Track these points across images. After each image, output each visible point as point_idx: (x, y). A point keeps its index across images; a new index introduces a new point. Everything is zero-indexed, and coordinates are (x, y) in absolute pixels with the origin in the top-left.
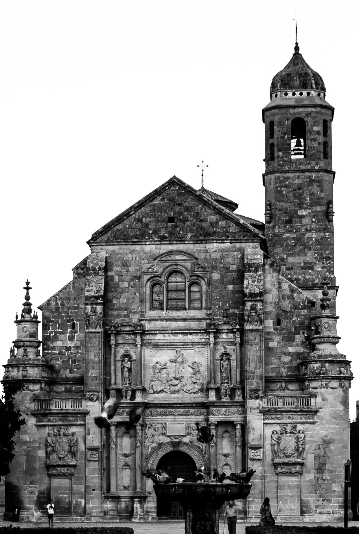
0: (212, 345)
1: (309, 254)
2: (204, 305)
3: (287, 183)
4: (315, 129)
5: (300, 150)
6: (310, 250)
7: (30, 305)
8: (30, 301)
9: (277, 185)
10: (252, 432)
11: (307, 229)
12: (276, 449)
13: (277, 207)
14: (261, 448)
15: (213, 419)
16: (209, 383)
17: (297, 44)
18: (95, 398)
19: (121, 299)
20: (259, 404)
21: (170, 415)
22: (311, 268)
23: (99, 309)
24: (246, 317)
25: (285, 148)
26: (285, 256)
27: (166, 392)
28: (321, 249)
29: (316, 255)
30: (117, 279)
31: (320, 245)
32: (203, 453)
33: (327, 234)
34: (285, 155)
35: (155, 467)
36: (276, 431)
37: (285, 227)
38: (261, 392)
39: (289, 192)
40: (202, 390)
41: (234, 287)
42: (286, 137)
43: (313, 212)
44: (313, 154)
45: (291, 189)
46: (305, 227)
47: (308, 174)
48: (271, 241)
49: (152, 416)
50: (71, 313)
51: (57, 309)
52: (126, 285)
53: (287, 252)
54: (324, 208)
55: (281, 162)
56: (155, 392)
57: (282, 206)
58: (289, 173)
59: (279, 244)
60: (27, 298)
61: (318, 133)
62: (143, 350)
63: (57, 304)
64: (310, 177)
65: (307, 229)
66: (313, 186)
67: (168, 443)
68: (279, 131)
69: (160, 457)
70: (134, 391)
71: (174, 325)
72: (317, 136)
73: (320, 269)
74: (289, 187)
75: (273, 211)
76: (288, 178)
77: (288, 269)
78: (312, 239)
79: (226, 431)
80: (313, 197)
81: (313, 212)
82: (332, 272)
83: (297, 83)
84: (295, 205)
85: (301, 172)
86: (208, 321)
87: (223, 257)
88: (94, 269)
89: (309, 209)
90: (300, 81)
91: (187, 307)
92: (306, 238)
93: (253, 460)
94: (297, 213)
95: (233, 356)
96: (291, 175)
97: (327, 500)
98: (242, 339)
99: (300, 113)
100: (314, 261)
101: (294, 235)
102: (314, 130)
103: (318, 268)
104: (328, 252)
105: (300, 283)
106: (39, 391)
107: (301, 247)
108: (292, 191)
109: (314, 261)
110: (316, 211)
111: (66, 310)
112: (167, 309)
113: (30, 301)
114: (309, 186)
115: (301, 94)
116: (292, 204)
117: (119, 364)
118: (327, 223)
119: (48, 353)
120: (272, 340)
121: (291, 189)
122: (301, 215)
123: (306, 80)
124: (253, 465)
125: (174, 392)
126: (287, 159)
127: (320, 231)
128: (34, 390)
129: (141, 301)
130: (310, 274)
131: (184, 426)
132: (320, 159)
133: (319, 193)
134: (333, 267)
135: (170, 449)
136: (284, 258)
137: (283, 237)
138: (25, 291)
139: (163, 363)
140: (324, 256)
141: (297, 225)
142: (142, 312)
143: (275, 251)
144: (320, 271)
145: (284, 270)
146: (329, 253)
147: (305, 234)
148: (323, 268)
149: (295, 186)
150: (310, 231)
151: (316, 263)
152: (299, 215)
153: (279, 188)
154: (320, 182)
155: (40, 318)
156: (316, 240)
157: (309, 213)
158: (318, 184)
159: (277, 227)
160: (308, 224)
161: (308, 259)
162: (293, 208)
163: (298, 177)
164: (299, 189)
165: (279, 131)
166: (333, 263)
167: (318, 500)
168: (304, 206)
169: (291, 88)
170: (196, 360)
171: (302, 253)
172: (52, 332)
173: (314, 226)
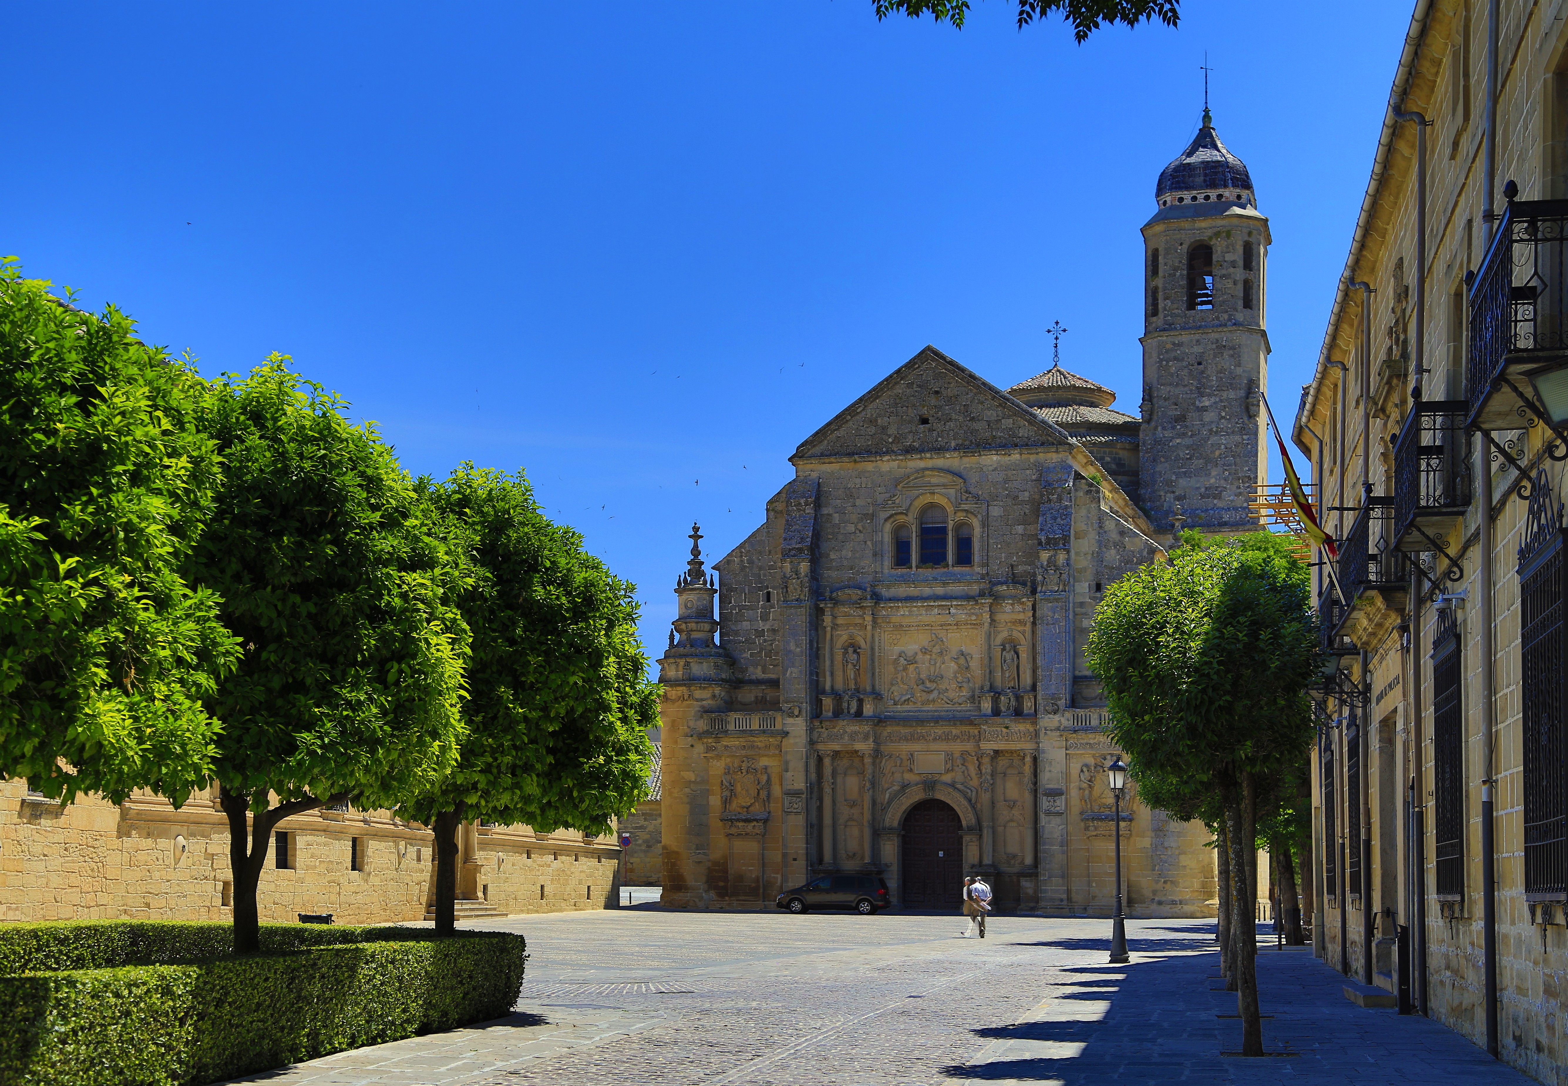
0: (986, 625)
1: (1214, 473)
2: (976, 558)
4: (1229, 257)
5: (1207, 295)
7: (702, 563)
8: (701, 558)
10: (1047, 769)
11: (1211, 430)
12: (1087, 797)
14: (1061, 794)
15: (988, 746)
16: (982, 688)
17: (1206, 111)
18: (796, 713)
19: (844, 552)
20: (1060, 721)
21: (919, 739)
22: (1218, 496)
23: (804, 567)
24: (1039, 578)
26: (1174, 478)
27: (915, 703)
29: (1227, 473)
30: (836, 518)
31: (1233, 456)
32: (973, 801)
34: (1175, 306)
35: (895, 824)
36: (1087, 765)
37: (1174, 428)
38: (1063, 701)
40: (972, 698)
41: (1025, 530)
42: (1178, 274)
43: (1221, 401)
44: (1224, 302)
46: (1206, 428)
49: (892, 741)
50: (765, 575)
51: (743, 568)
52: (851, 528)
54: (1242, 393)
56: (895, 704)
59: (1163, 456)
60: (696, 551)
61: (1233, 264)
62: (876, 635)
63: (742, 561)
64: (1217, 341)
67: (916, 784)
68: (1166, 264)
69: (904, 808)
70: (860, 702)
71: (927, 591)
72: (1232, 270)
74: (1183, 360)
75: (1155, 400)
76: (1180, 345)
77: (1179, 498)
79: (1011, 766)
83: (1199, 180)
86: (982, 586)
87: (1006, 481)
88: (800, 504)
90: (1206, 175)
91: (950, 563)
93: (1049, 813)
94: (1194, 404)
95: (1023, 641)
96: (1185, 337)
97: (1172, 882)
98: (1034, 616)
106: (710, 702)
110: (1228, 399)
111: (756, 571)
112: (917, 567)
113: (701, 558)
114: (1215, 356)
115: (1207, 198)
116: (1186, 389)
117: (839, 657)
119: (729, 641)
120: (1086, 614)
121: (1184, 364)
123: (1216, 173)
124: (1049, 822)
125: (928, 702)
128: (702, 700)
129: (875, 555)
131: (943, 756)
132: (1236, 310)
135: (917, 795)
136: (1172, 481)
138: (692, 541)
139: (910, 654)
142: (876, 572)
150: (1216, 433)
155: (716, 586)
157: (1215, 403)
158: (1231, 352)
159: (1160, 428)
161: (1213, 481)
164: (1200, 364)
165: (1166, 264)
167: (1157, 882)
169: (1188, 188)
170: (963, 648)
172: (734, 607)
173: (1224, 423)
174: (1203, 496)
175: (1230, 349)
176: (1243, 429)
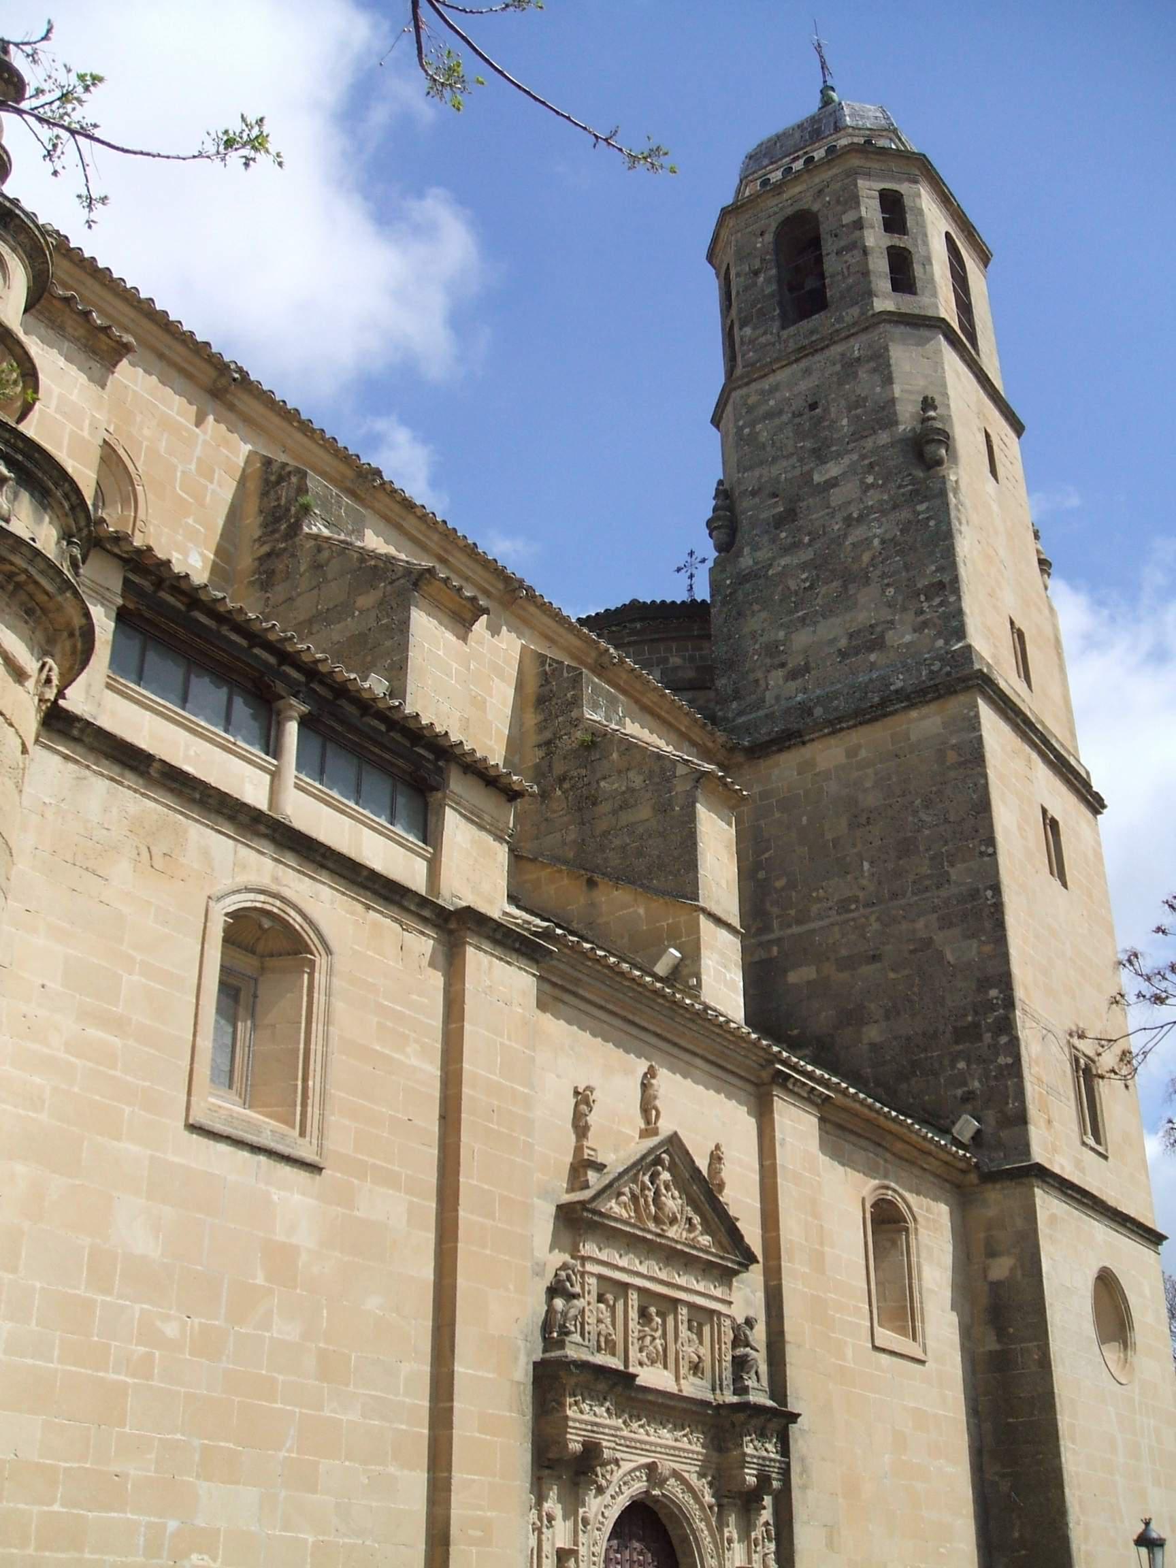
3: (772, 403)
6: (867, 581)
9: (741, 423)
13: (743, 488)
22: (877, 644)
25: (761, 313)
26: (781, 634)
28: (907, 567)
31: (898, 553)
33: (921, 508)
34: (761, 331)
39: (780, 429)
42: (761, 279)
43: (863, 457)
44: (849, 289)
45: (785, 418)
47: (837, 349)
48: (729, 603)
53: (785, 620)
55: (751, 354)
57: (761, 476)
58: (774, 371)
64: (843, 355)
65: (849, 521)
66: (855, 375)
72: (857, 233)
73: (908, 638)
76: (775, 389)
77: (793, 675)
78: (872, 542)
80: (859, 411)
81: (863, 457)
82: (960, 633)
84: (801, 460)
85: (812, 354)
89: (848, 452)
92: (849, 549)
96: (782, 376)
99: (795, 200)
100: (886, 614)
101: (806, 555)
102: (844, 222)
103: (903, 637)
104: (933, 568)
105: (836, 709)
107: (835, 584)
108: (790, 421)
109: (886, 614)
114: (840, 384)
116: (794, 459)
118: (920, 474)
121: (785, 418)
122: (825, 482)
126: (769, 336)
127: (895, 507)
130: (873, 666)
133: (878, 389)
134: (960, 612)
137: (770, 572)
140: (919, 586)
141: (814, 516)
143: (746, 630)
144: (908, 645)
145: (781, 682)
146: (937, 571)
147: (845, 536)
148: (919, 629)
149: (798, 404)
150: (861, 519)
151: (892, 622)
152: (819, 484)
153: (747, 431)
154: (880, 356)
156: (883, 542)
157: (853, 465)
158: (873, 364)
160: (849, 503)
162: (797, 472)
163: (807, 372)
164: (813, 407)
166: (959, 598)
168: (834, 448)
171: (842, 602)
174: (843, 654)
175: (868, 361)
176: (916, 492)
